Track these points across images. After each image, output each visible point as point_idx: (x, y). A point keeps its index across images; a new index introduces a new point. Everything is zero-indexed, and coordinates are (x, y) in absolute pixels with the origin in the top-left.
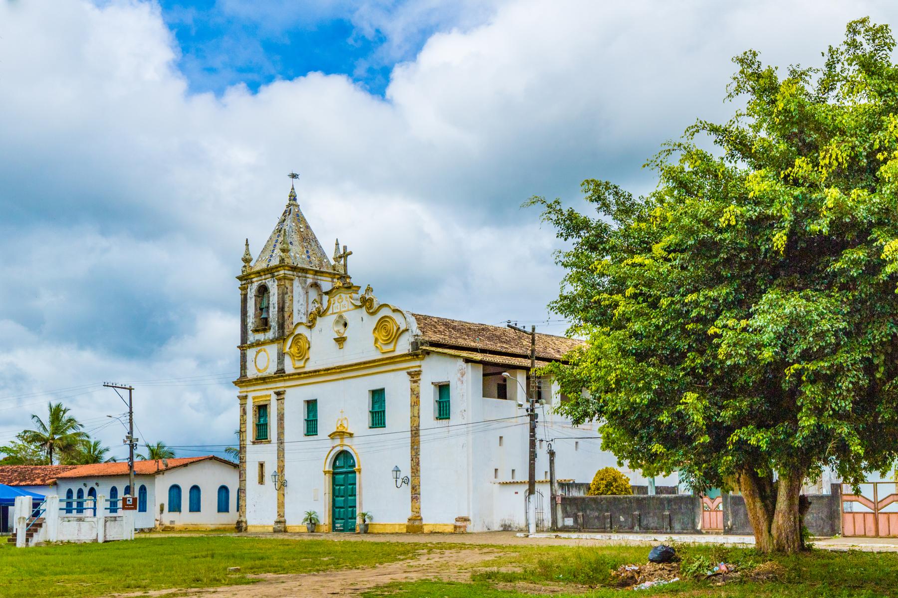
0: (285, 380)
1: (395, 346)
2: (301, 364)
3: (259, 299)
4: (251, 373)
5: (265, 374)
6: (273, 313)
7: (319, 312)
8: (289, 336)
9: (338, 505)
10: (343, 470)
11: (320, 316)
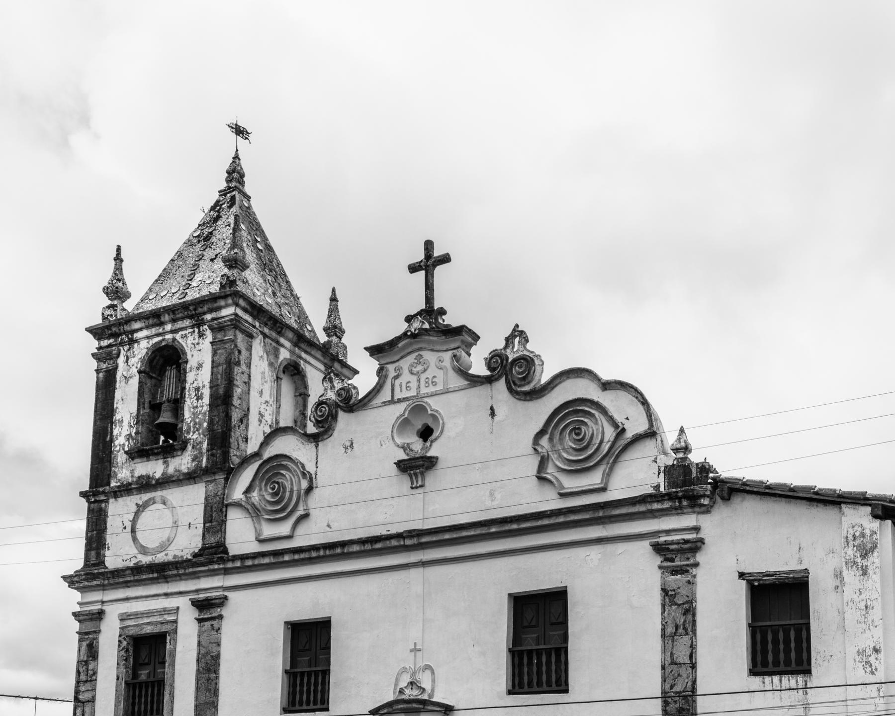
0: (227, 572)
1: (608, 475)
2: (284, 529)
3: (149, 383)
5: (160, 558)
6: (196, 409)
7: (348, 398)
8: (246, 461)
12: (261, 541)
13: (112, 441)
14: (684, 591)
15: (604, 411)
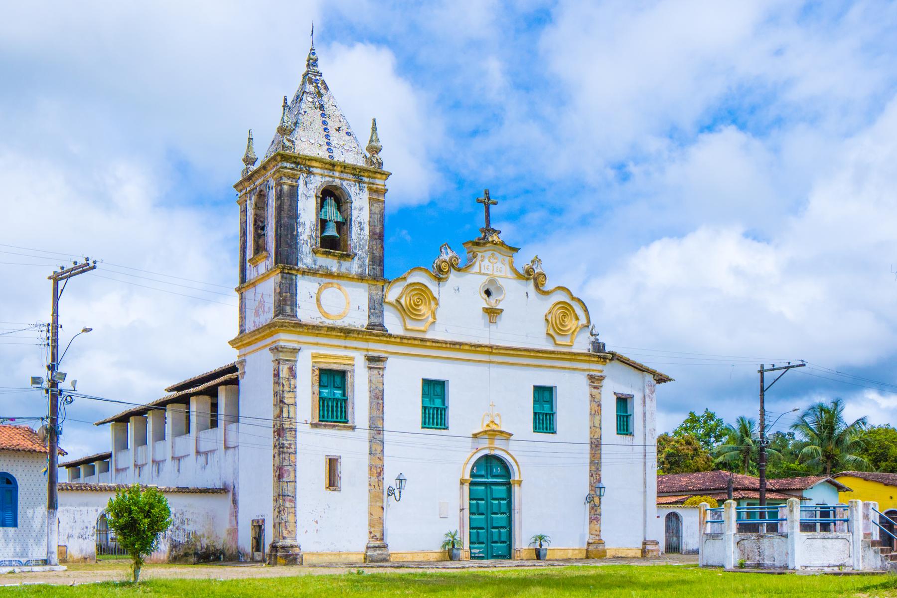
0: (388, 343)
4: (306, 312)
5: (339, 323)
6: (359, 235)
10: (492, 480)
11: (459, 270)
12: (407, 329)
13: (297, 235)
14: (598, 396)
15: (574, 311)
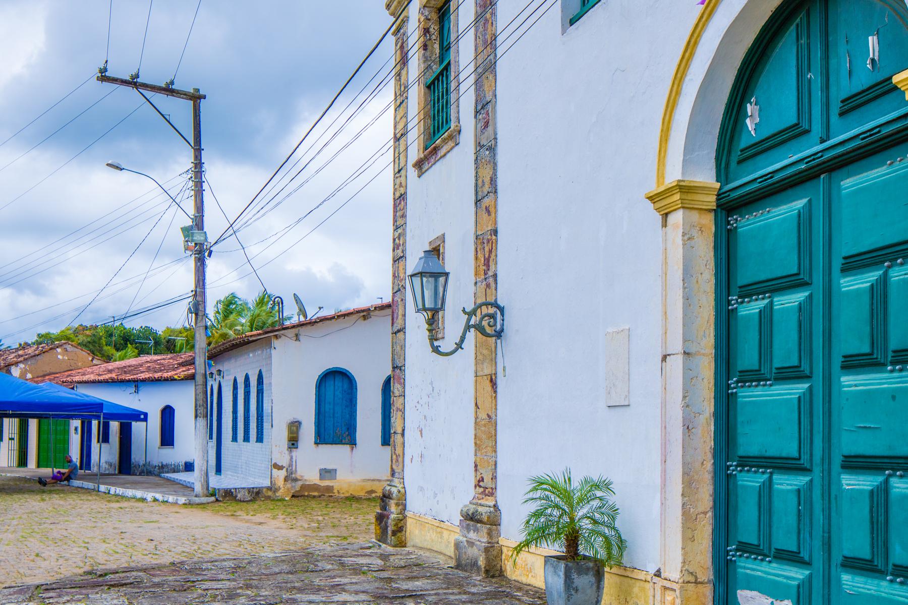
9: (751, 442)
